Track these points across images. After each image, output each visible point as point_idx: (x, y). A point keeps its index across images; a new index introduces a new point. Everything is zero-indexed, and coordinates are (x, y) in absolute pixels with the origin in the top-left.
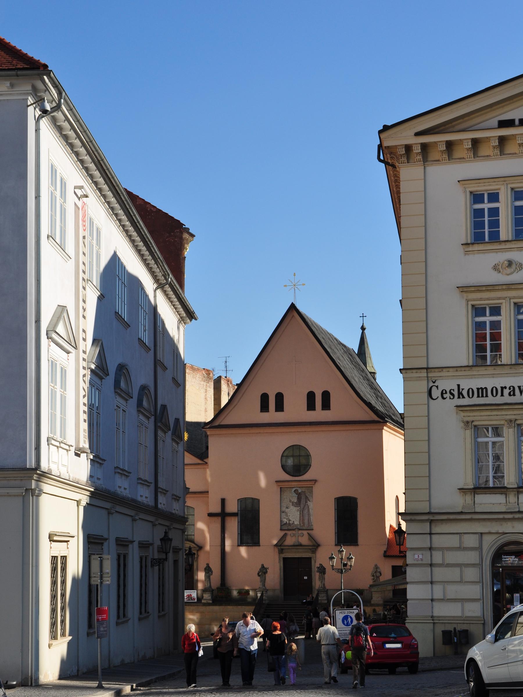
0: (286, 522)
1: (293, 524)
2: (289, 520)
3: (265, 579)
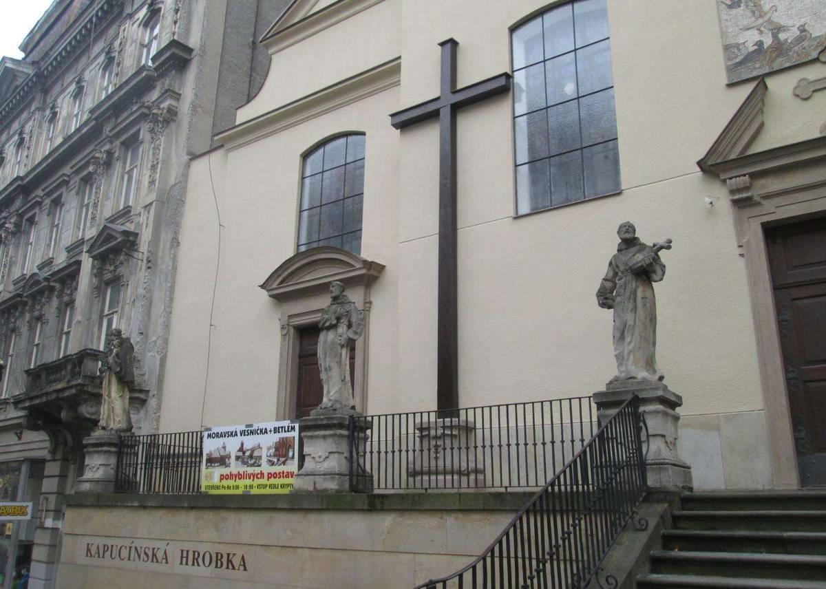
0: (760, 44)
1: (800, 39)
2: (777, 29)
3: (653, 319)
